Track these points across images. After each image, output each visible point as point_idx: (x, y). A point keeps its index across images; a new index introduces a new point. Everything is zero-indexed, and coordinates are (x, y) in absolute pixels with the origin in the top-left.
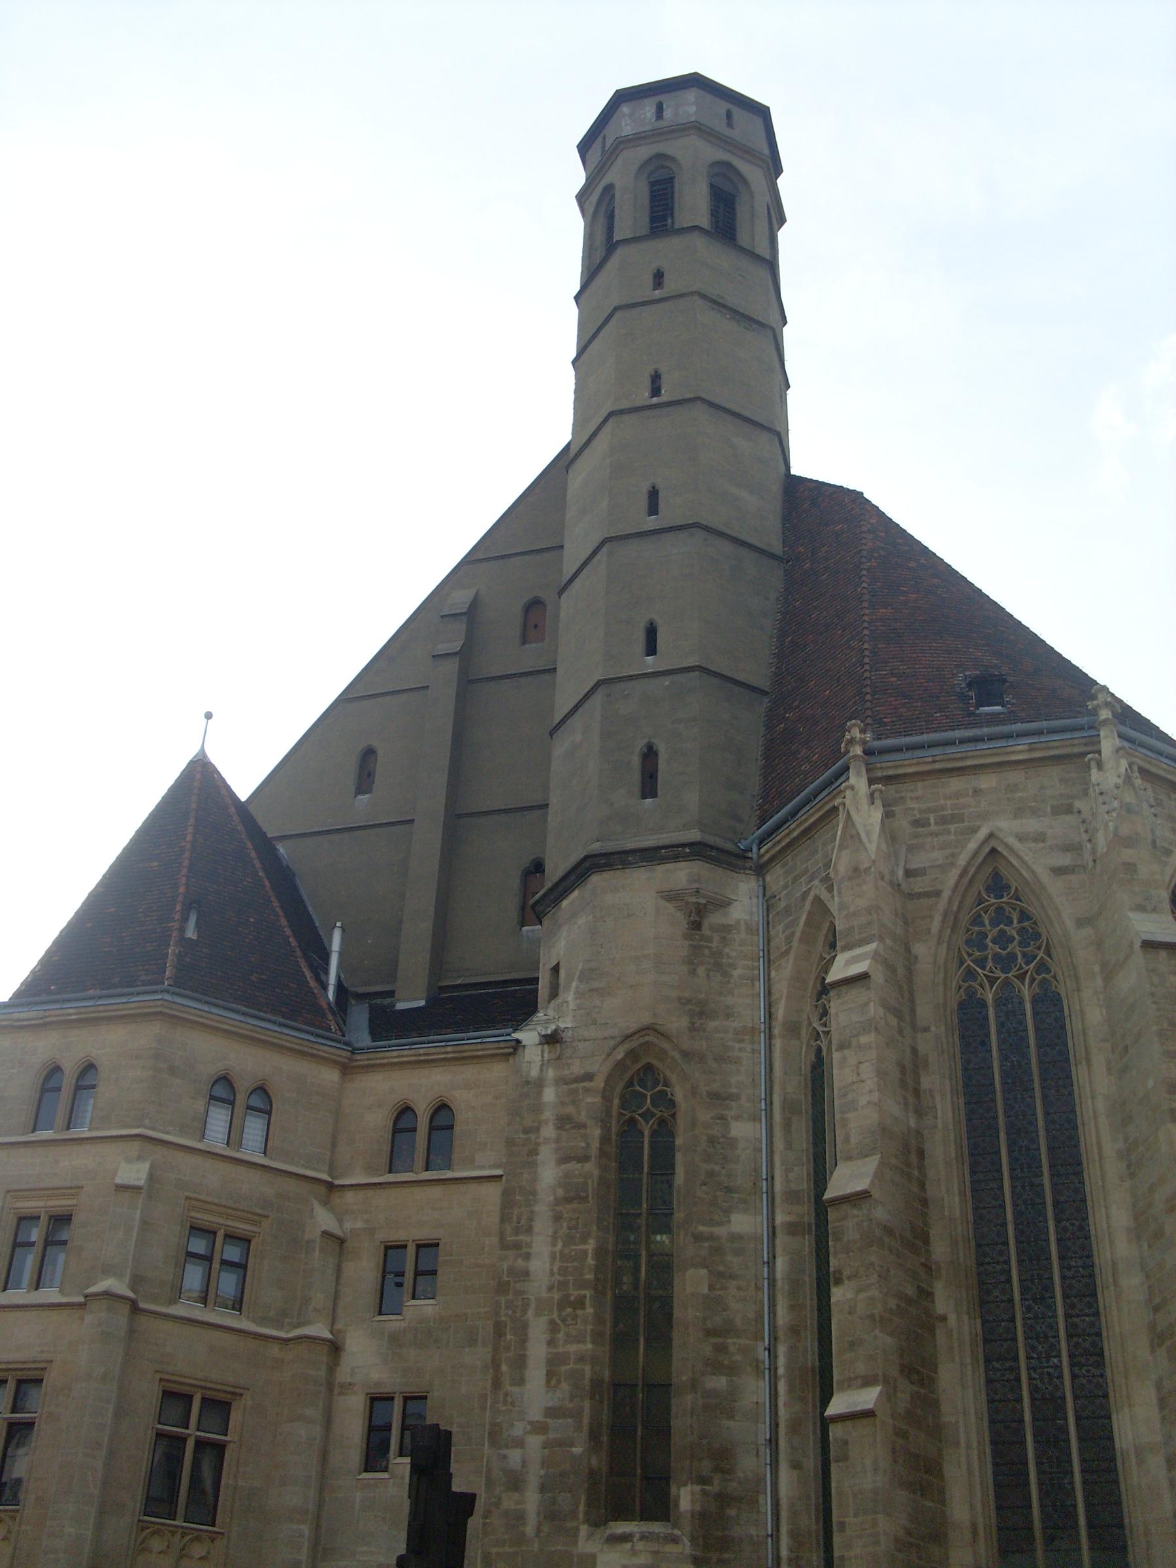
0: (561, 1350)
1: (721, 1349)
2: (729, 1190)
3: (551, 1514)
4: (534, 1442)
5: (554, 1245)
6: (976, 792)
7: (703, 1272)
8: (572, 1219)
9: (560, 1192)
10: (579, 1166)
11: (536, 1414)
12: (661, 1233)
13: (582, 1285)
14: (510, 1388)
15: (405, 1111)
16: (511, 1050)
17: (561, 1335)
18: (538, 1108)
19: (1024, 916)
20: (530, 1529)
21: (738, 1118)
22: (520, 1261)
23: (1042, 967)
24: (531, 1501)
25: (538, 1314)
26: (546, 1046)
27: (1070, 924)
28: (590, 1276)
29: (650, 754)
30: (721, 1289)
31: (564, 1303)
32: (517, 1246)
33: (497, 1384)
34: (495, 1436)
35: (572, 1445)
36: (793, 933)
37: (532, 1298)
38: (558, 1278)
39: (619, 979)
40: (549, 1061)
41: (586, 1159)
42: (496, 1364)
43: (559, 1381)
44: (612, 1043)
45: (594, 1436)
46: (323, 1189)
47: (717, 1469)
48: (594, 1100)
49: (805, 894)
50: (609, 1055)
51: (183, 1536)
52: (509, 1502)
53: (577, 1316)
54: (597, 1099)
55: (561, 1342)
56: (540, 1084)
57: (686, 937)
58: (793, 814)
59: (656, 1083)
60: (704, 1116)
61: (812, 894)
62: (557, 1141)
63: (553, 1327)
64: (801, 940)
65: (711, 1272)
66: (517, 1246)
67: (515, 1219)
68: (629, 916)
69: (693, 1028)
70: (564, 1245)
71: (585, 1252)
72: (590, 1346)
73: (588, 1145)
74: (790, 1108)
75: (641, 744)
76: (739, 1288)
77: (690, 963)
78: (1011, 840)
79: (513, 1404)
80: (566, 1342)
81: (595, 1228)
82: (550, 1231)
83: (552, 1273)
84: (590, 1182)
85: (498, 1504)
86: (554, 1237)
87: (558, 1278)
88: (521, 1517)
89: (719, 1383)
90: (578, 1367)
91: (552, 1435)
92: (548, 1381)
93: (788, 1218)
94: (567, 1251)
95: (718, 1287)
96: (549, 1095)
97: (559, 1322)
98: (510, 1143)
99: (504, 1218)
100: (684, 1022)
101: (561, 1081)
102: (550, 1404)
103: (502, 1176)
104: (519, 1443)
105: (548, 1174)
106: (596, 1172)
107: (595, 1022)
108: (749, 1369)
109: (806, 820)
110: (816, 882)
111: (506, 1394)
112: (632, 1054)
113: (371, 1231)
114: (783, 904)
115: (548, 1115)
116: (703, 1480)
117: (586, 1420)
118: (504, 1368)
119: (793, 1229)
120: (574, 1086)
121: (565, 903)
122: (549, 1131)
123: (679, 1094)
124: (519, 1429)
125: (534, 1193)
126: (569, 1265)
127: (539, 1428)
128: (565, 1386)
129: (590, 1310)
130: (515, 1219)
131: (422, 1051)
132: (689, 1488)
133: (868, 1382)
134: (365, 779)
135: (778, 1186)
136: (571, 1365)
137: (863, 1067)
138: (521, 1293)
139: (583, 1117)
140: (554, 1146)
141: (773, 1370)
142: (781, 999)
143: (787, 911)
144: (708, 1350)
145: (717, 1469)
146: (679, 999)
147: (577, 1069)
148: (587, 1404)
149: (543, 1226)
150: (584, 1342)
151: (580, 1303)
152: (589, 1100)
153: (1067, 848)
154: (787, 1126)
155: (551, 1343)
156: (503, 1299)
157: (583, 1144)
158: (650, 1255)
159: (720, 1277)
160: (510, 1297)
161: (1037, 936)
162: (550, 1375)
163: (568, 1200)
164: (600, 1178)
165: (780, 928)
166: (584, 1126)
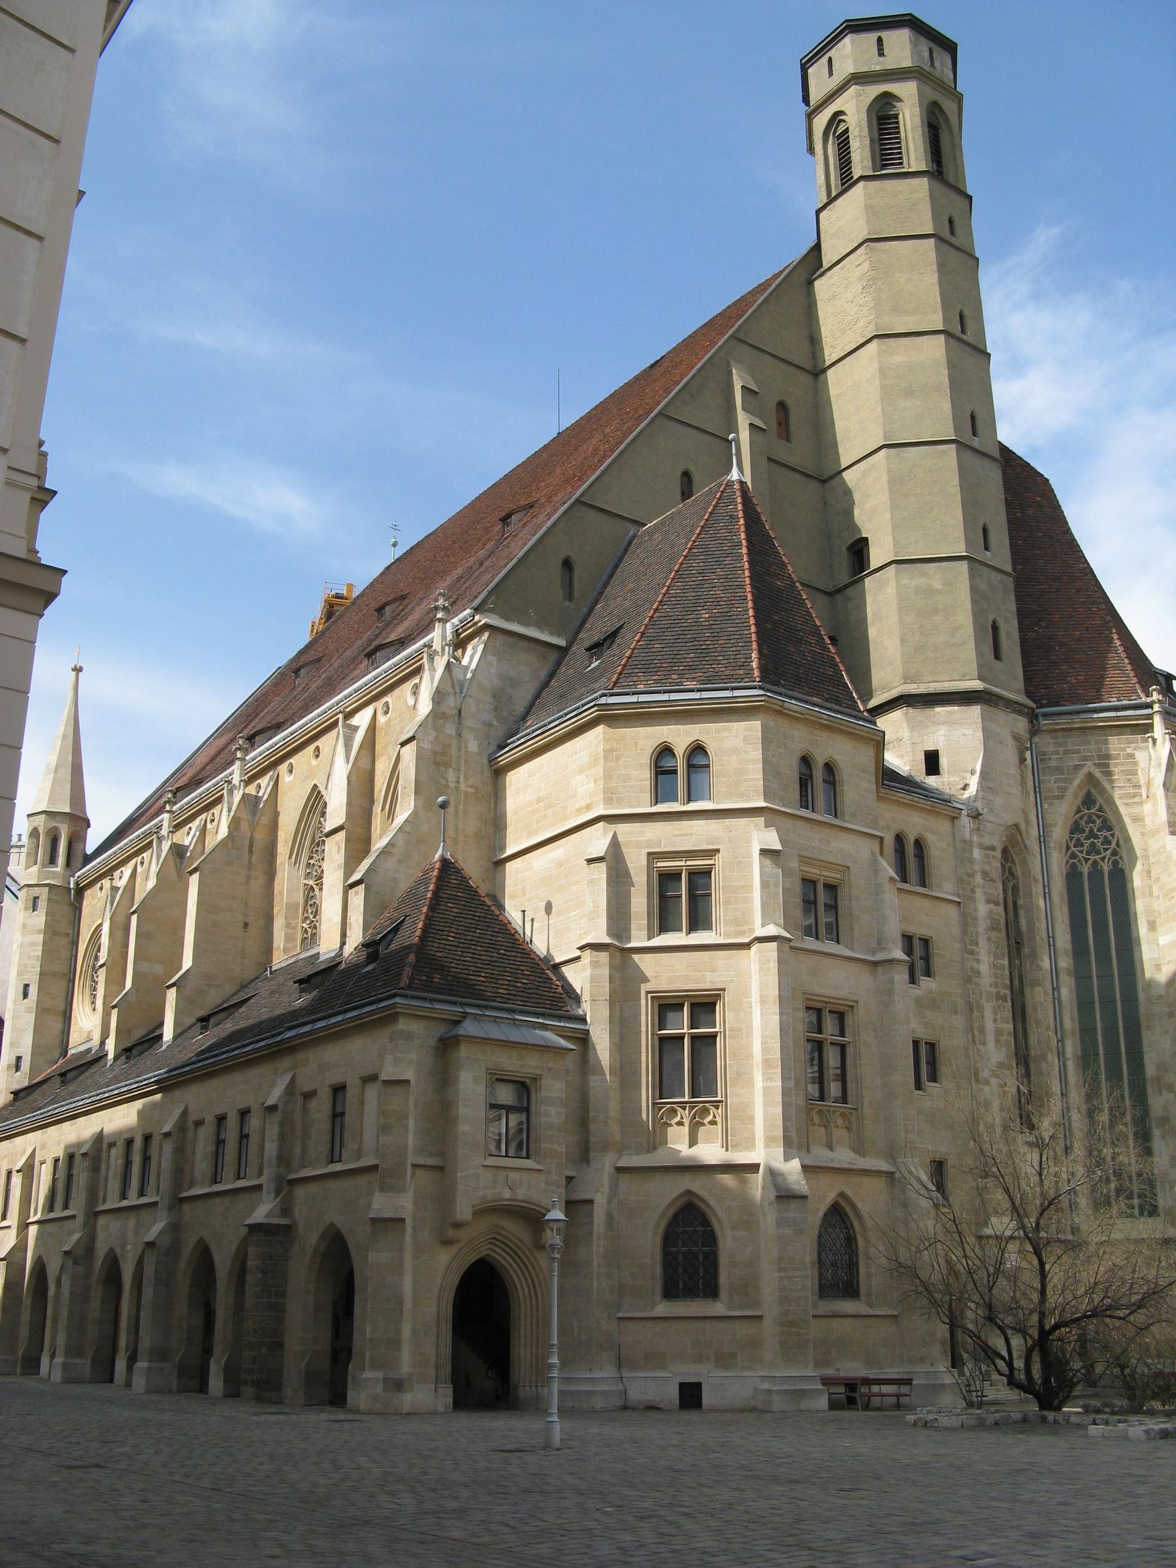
3: (1006, 1128)
8: (995, 942)
15: (899, 839)
17: (998, 1017)
18: (971, 861)
25: (988, 1001)
29: (995, 628)
32: (972, 953)
33: (974, 1042)
34: (976, 1074)
36: (1066, 788)
41: (997, 904)
44: (1002, 828)
49: (1078, 768)
51: (692, 1108)
57: (1020, 768)
58: (1078, 712)
61: (1085, 770)
63: (995, 1013)
66: (972, 953)
71: (1003, 965)
82: (987, 947)
88: (992, 1126)
96: (977, 853)
98: (960, 881)
99: (965, 932)
103: (959, 903)
105: (982, 909)
109: (1088, 722)
110: (1090, 763)
111: (978, 1050)
114: (1054, 763)
120: (988, 852)
121: (938, 709)
122: (978, 879)
123: (1018, 871)
124: (985, 1074)
125: (975, 919)
128: (1003, 1049)
129: (1010, 1004)
131: (916, 799)
135: (1059, 944)
138: (977, 985)
142: (1055, 825)
147: (987, 840)
155: (995, 1020)
159: (1045, 993)
162: (997, 1041)
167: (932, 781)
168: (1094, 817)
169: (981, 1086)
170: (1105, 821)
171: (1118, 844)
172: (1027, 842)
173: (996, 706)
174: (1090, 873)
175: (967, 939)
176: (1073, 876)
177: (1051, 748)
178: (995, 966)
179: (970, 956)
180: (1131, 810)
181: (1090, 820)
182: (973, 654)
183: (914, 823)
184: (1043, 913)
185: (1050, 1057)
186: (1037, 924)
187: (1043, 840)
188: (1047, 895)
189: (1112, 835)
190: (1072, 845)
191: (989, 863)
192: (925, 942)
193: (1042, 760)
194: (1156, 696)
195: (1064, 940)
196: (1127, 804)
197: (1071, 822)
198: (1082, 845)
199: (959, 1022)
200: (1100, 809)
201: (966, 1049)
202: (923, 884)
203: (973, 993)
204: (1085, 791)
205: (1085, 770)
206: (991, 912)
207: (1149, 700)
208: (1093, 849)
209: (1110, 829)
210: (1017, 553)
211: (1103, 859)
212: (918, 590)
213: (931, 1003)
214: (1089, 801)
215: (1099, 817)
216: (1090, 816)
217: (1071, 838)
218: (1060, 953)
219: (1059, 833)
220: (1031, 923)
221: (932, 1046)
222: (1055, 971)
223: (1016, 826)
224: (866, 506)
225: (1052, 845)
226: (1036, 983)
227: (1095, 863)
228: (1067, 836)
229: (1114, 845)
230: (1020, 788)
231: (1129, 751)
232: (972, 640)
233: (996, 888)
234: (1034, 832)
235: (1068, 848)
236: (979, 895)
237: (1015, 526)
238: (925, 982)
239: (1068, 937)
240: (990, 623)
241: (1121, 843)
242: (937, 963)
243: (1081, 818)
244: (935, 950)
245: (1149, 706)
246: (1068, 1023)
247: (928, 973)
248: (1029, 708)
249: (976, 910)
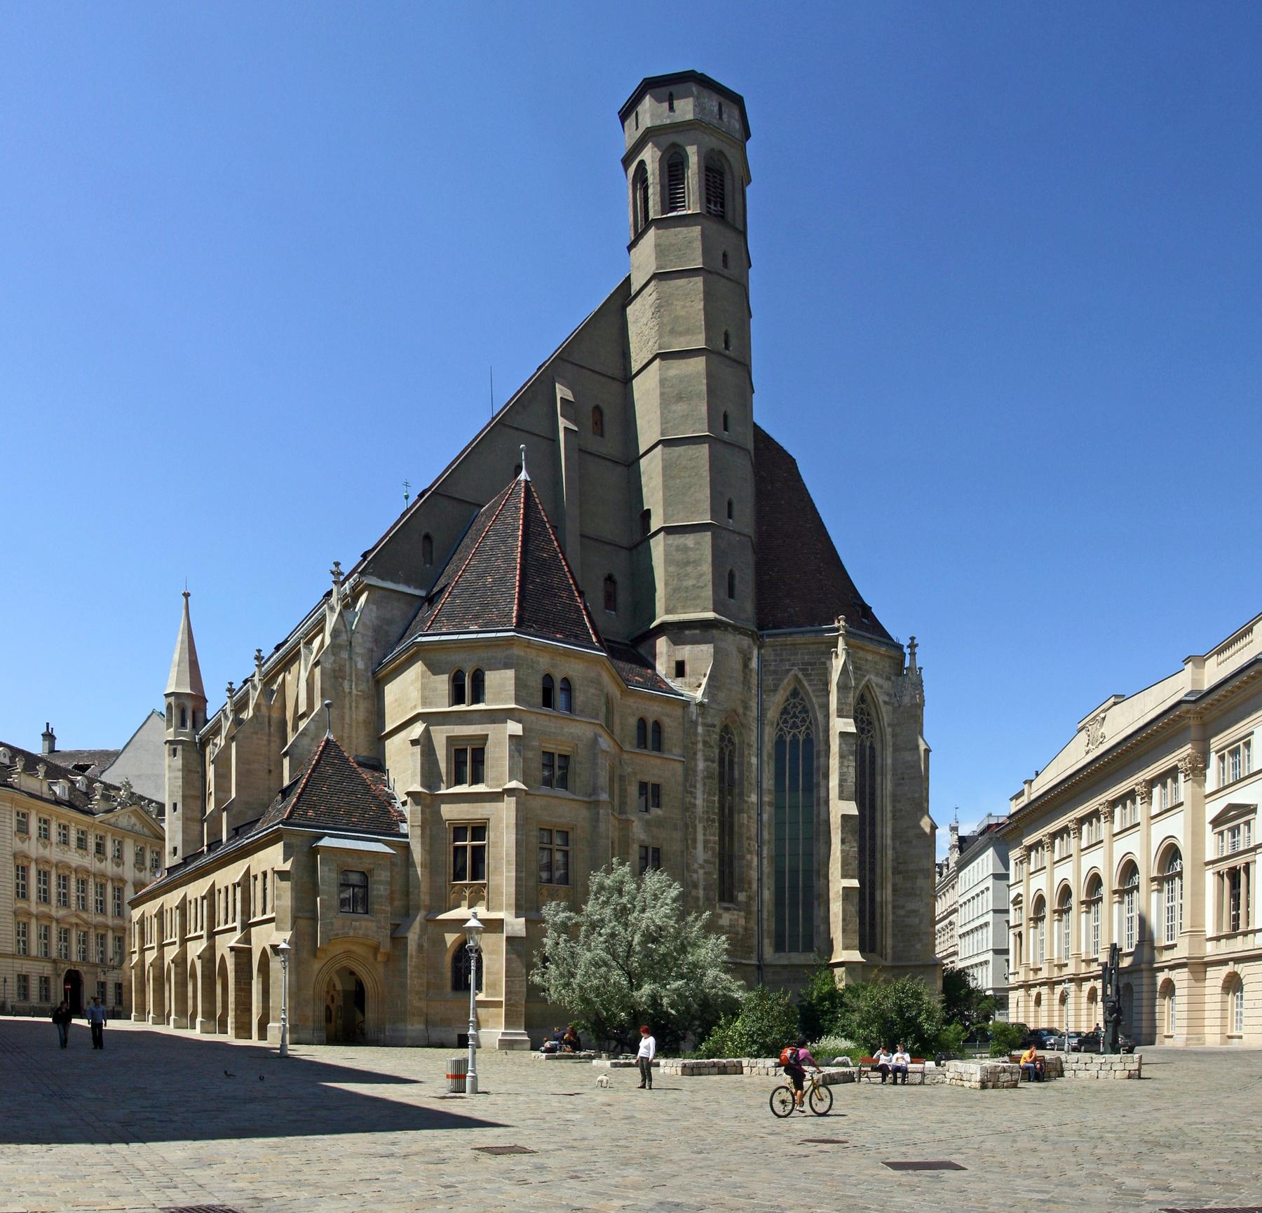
1: (749, 845)
3: (707, 899)
4: (701, 872)
6: (866, 660)
7: (745, 815)
9: (705, 773)
11: (701, 861)
13: (714, 813)
15: (642, 722)
18: (696, 734)
19: (868, 715)
20: (701, 903)
22: (693, 800)
23: (872, 737)
24: (701, 893)
25: (700, 822)
27: (886, 724)
29: (731, 575)
31: (708, 819)
33: (687, 848)
34: (688, 867)
36: (779, 685)
41: (713, 762)
48: (716, 737)
49: (788, 671)
52: (694, 893)
56: (695, 724)
58: (791, 634)
60: (746, 753)
61: (792, 672)
63: (705, 828)
66: (691, 793)
74: (769, 756)
77: (744, 684)
78: (874, 685)
85: (690, 893)
86: (704, 791)
88: (697, 899)
96: (700, 729)
98: (686, 747)
99: (686, 780)
101: (704, 725)
103: (684, 762)
104: (696, 872)
106: (717, 768)
110: (796, 668)
114: (772, 668)
115: (700, 738)
119: (770, 804)
121: (687, 632)
122: (700, 746)
123: (736, 740)
124: (696, 866)
125: (696, 771)
127: (702, 867)
128: (710, 852)
129: (717, 824)
133: (852, 877)
135: (765, 786)
139: (712, 744)
141: (761, 855)
143: (775, 672)
147: (709, 720)
148: (717, 860)
149: (699, 786)
151: (713, 821)
153: (888, 694)
155: (704, 835)
159: (749, 817)
161: (870, 723)
162: (705, 847)
163: (708, 777)
165: (771, 678)
167: (676, 684)
170: (804, 707)
171: (810, 723)
172: (745, 721)
173: (726, 630)
174: (791, 741)
176: (780, 743)
177: (772, 658)
178: (708, 801)
180: (820, 700)
181: (795, 706)
182: (711, 593)
183: (653, 711)
184: (754, 768)
185: (749, 857)
186: (746, 774)
187: (761, 719)
188: (759, 755)
189: (808, 716)
190: (781, 723)
191: (709, 735)
192: (657, 787)
193: (765, 666)
194: (842, 623)
195: (768, 783)
196: (817, 696)
197: (781, 707)
198: (788, 722)
199: (677, 835)
200: (802, 699)
201: (683, 852)
202: (659, 750)
204: (792, 687)
206: (708, 767)
207: (836, 625)
208: (795, 726)
209: (807, 712)
210: (760, 517)
211: (800, 732)
212: (678, 549)
213: (660, 823)
214: (795, 693)
215: (800, 704)
216: (795, 704)
217: (781, 718)
219: (772, 714)
220: (741, 773)
221: (657, 851)
222: (761, 803)
223: (735, 711)
224: (651, 485)
225: (766, 722)
226: (741, 811)
227: (794, 735)
228: (778, 716)
229: (807, 723)
230: (742, 686)
231: (823, 660)
232: (711, 584)
233: (714, 753)
234: (754, 713)
235: (778, 725)
236: (700, 755)
237: (761, 496)
238: (656, 812)
239: (772, 782)
240: (728, 572)
242: (664, 799)
243: (789, 705)
244: (663, 792)
245: (837, 630)
246: (766, 836)
247: (658, 805)
248: (752, 631)
249: (696, 765)
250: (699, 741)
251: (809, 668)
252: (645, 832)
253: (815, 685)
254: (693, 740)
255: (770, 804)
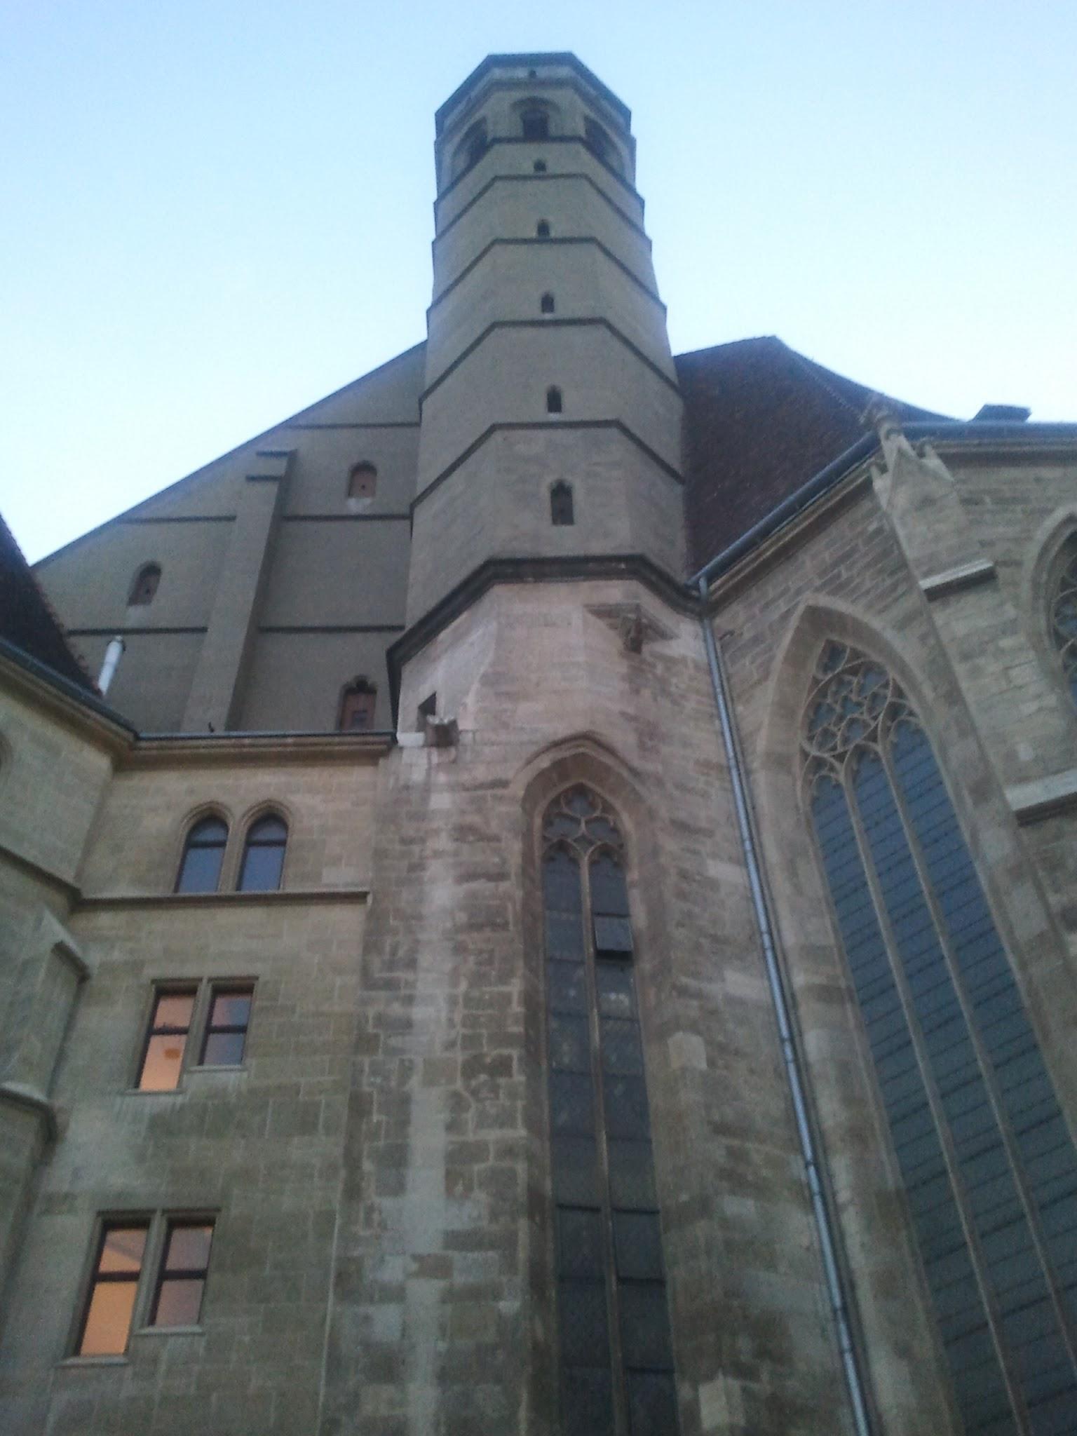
0: (471, 1137)
1: (736, 1155)
2: (715, 939)
4: (426, 1292)
5: (455, 984)
8: (481, 952)
9: (462, 917)
10: (491, 885)
12: (617, 991)
13: (509, 1040)
14: (377, 1200)
16: (383, 747)
17: (470, 1116)
18: (420, 816)
21: (714, 856)
25: (429, 1082)
26: (435, 752)
28: (517, 1029)
30: (726, 1067)
32: (390, 985)
33: (353, 1192)
35: (497, 1296)
37: (419, 1061)
38: (463, 1031)
39: (538, 684)
40: (439, 765)
41: (501, 876)
42: (352, 1161)
43: (469, 1189)
44: (534, 749)
45: (536, 1283)
46: (60, 900)
47: (763, 1353)
50: (529, 762)
53: (498, 1086)
54: (516, 810)
55: (471, 1126)
56: (427, 789)
59: (592, 806)
60: (671, 845)
62: (456, 854)
63: (457, 1103)
64: (786, 659)
65: (709, 1043)
66: (390, 985)
67: (387, 949)
68: (546, 625)
69: (642, 746)
70: (471, 985)
71: (507, 998)
72: (522, 1132)
73: (504, 861)
75: (549, 479)
76: (752, 1071)
79: (383, 1226)
80: (480, 1125)
81: (520, 964)
82: (448, 966)
83: (451, 1022)
84: (510, 907)
86: (455, 976)
87: (463, 1031)
89: (740, 1207)
90: (506, 1164)
91: (459, 1280)
92: (449, 1190)
93: (818, 980)
94: (475, 993)
95: (720, 1063)
96: (441, 801)
97: (466, 1094)
98: (380, 854)
100: (632, 739)
102: (457, 1226)
106: (519, 894)
107: (505, 726)
108: (786, 1193)
111: (370, 1210)
112: (559, 765)
113: (136, 967)
114: (747, 635)
116: (744, 1372)
117: (522, 1254)
118: (367, 1166)
119: (826, 994)
120: (480, 793)
122: (443, 842)
125: (419, 917)
126: (480, 1012)
129: (519, 1078)
130: (387, 949)
132: (721, 1381)
134: (147, 578)
135: (790, 938)
136: (491, 1162)
137: (1014, 673)
139: (494, 827)
140: (451, 860)
141: (828, 1196)
142: (758, 729)
143: (756, 640)
144: (720, 1156)
145: (763, 1353)
146: (623, 714)
147: (481, 773)
148: (523, 1225)
150: (513, 1125)
151: (502, 1067)
152: (503, 809)
154: (791, 869)
155: (451, 1127)
156: (366, 1061)
157: (496, 860)
158: (605, 1018)
160: (380, 1056)
162: (451, 1177)
163: (472, 927)
164: (525, 904)
165: (747, 661)
166: (497, 839)
168: (847, 678)
169: (365, 1309)
175: (376, 962)
179: (383, 994)
191: (479, 811)
196: (880, 612)
203: (374, 1073)
205: (801, 609)
206: (473, 895)
211: (873, 738)
217: (811, 739)
218: (793, 958)
220: (657, 911)
222: (791, 1004)
225: (755, 765)
228: (800, 738)
230: (625, 686)
231: (872, 527)
236: (435, 868)
241: (903, 685)
246: (830, 1108)
250: (437, 832)
251: (842, 568)
252: (141, 1158)
253: (868, 592)
254: (412, 833)
255: (826, 994)
